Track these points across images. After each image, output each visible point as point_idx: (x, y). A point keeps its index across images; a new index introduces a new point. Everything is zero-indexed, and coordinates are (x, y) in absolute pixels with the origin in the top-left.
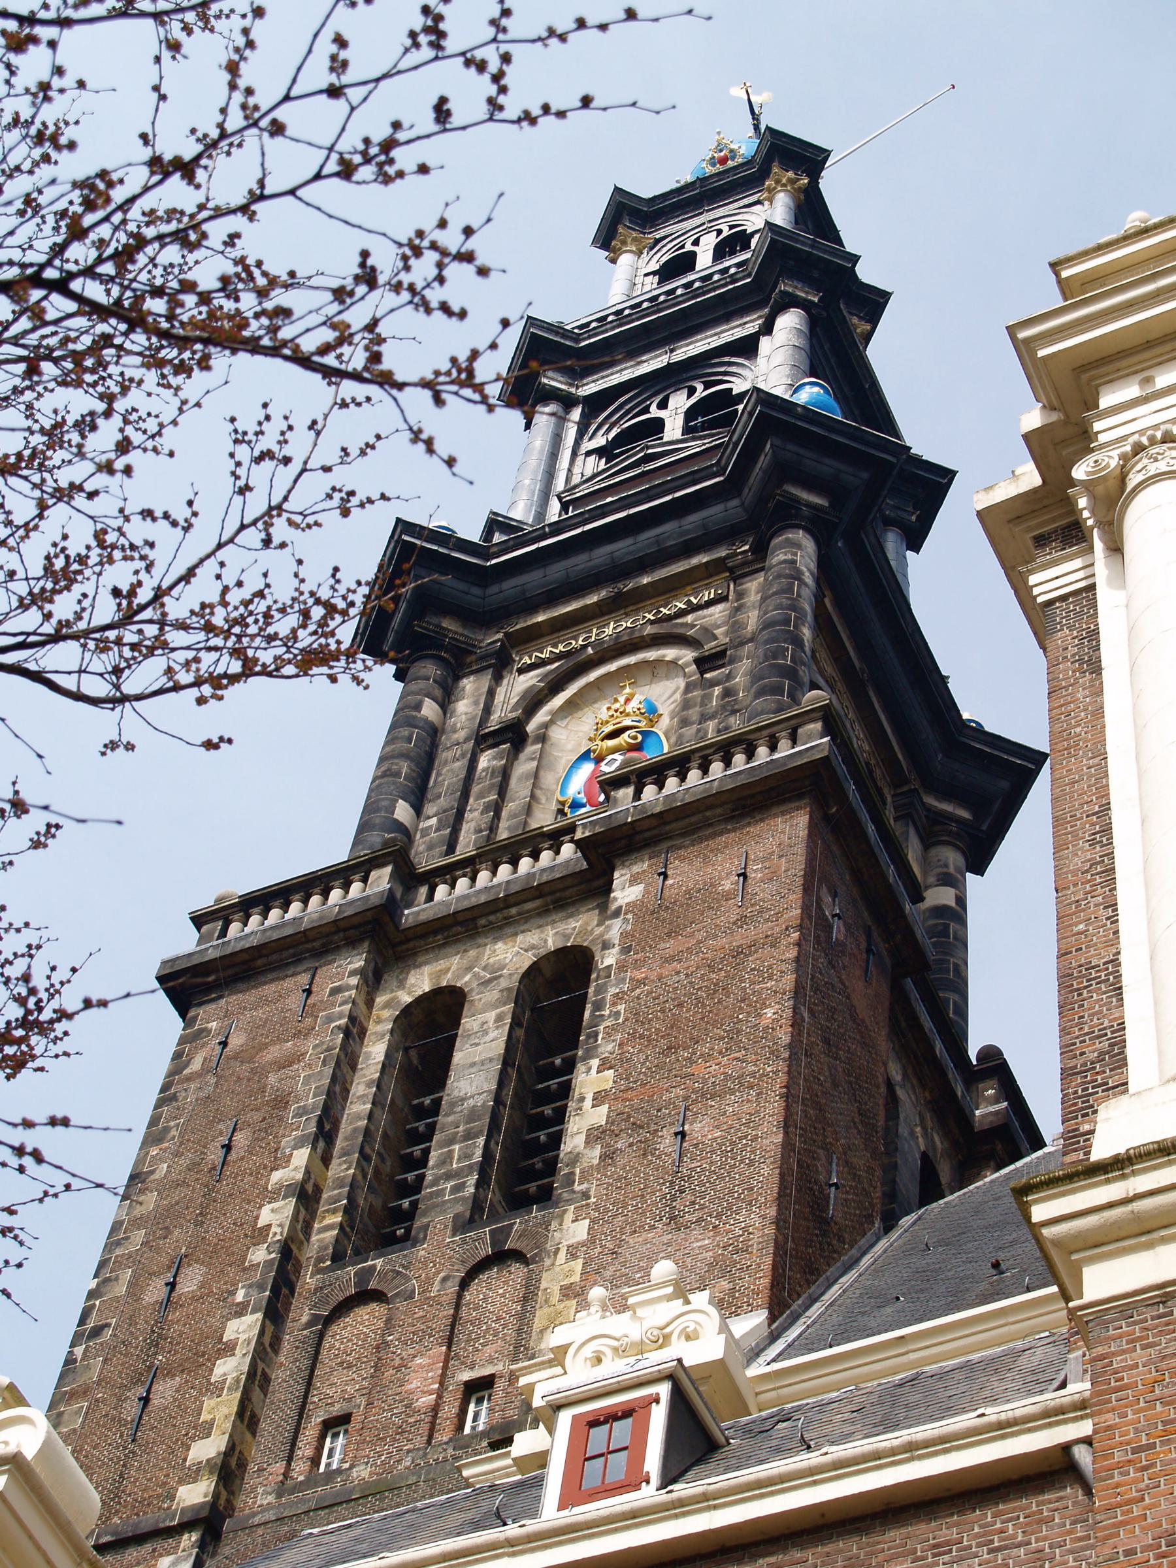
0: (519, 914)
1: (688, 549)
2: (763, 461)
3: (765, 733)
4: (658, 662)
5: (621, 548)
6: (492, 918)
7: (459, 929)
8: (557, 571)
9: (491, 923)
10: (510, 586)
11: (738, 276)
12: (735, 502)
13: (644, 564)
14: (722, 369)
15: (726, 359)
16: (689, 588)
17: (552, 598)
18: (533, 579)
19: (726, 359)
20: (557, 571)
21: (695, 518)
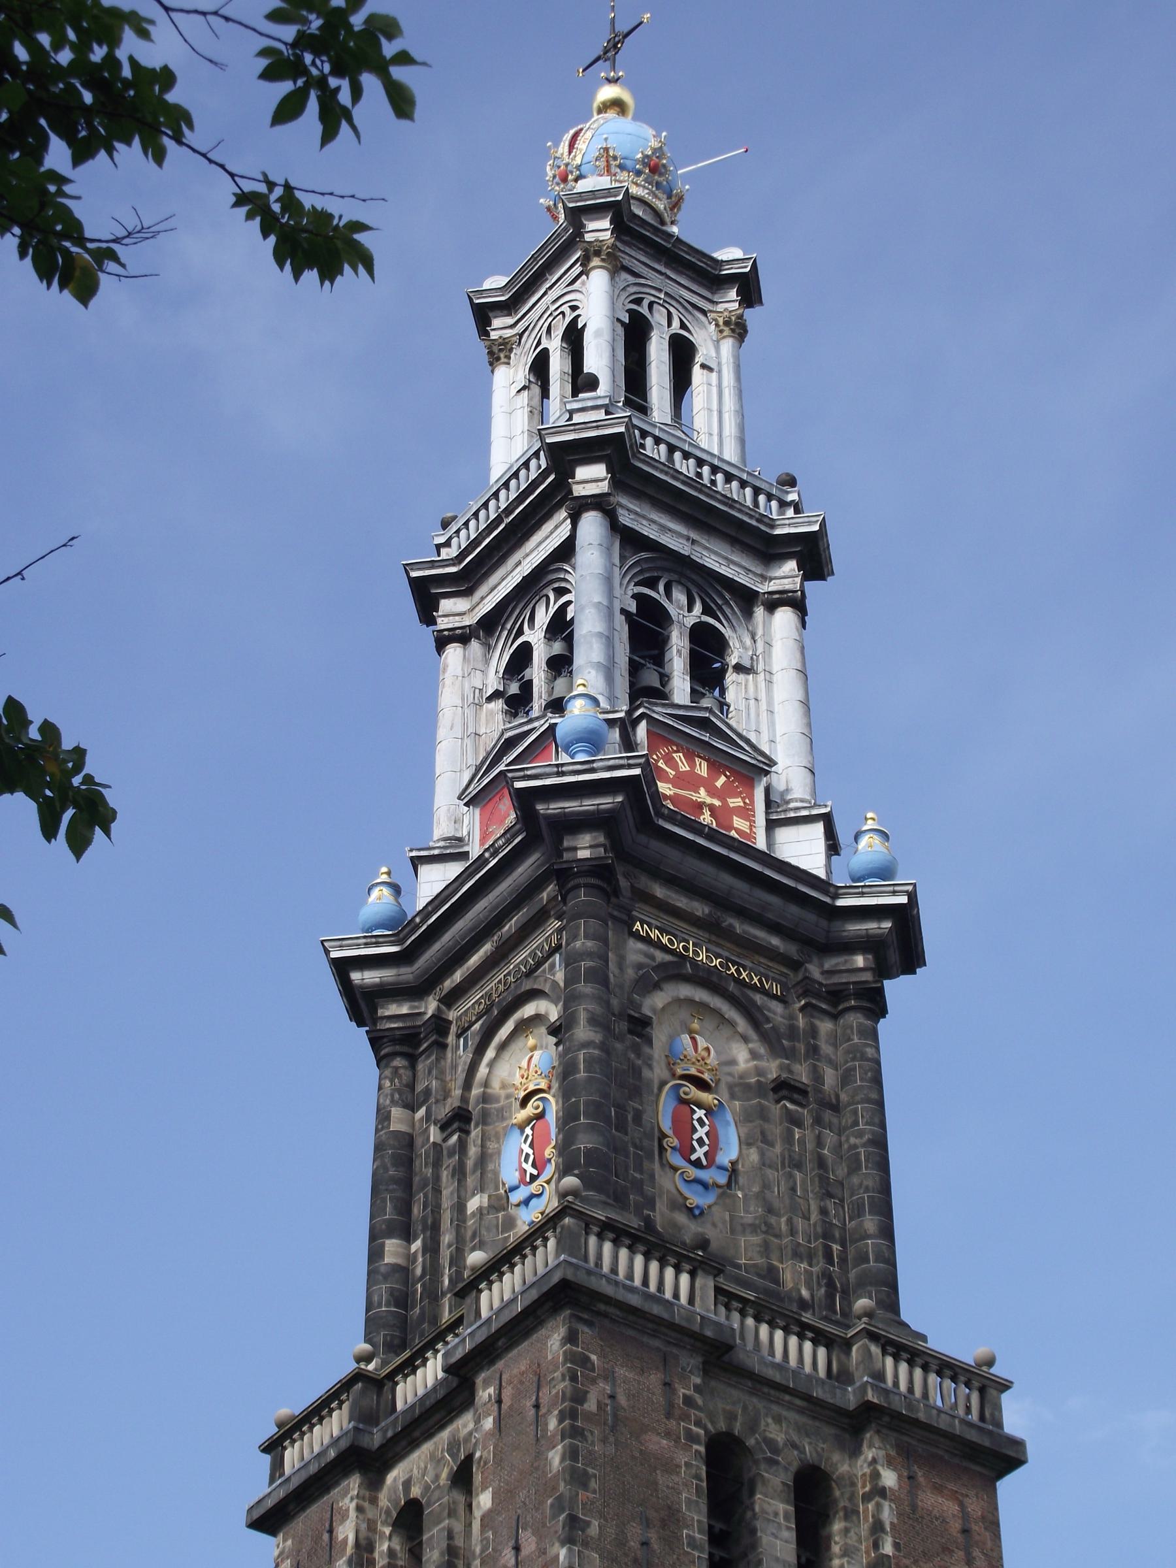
0: (789, 1402)
1: (775, 928)
2: (871, 926)
3: (968, 1375)
4: (732, 1024)
5: (740, 886)
6: (772, 1392)
7: (750, 1384)
8: (693, 866)
9: (769, 1394)
10: (657, 846)
11: (766, 520)
12: (824, 923)
13: (743, 913)
14: (720, 602)
15: (728, 596)
16: (757, 957)
17: (672, 881)
18: (673, 855)
19: (728, 596)
20: (693, 866)
21: (794, 910)
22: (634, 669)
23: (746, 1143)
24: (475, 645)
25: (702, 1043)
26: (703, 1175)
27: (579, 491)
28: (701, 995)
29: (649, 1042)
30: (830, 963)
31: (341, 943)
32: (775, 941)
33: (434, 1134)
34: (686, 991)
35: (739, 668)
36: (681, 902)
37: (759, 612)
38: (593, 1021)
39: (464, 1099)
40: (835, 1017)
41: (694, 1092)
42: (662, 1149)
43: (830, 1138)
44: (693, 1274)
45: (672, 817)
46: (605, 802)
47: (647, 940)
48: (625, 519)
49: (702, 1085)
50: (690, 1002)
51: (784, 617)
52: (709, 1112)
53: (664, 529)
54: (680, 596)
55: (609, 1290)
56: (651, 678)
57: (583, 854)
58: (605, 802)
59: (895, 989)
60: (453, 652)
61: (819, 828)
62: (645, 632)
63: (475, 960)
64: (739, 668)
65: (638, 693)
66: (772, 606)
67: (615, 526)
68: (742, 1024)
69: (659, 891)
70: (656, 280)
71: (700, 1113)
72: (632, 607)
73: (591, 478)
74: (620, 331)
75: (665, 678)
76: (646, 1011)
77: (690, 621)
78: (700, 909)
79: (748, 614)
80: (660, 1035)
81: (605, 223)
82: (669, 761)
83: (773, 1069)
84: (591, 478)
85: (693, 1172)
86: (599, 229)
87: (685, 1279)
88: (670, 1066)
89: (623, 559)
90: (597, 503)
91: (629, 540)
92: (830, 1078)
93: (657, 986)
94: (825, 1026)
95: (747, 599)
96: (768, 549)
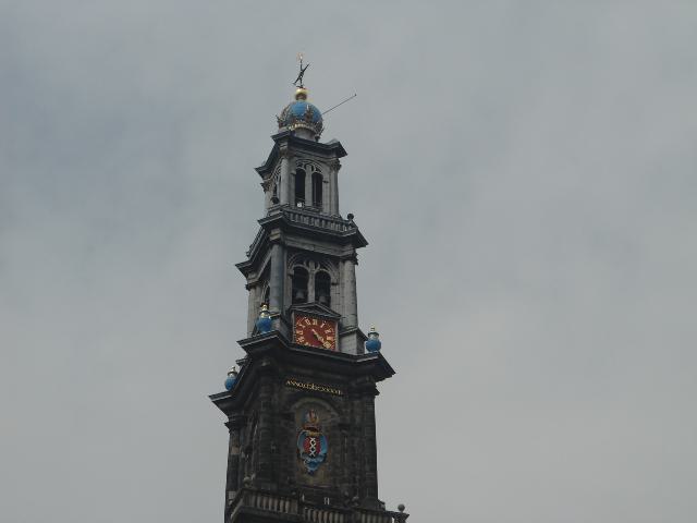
4: (324, 407)
22: (294, 293)
23: (330, 446)
24: (258, 289)
25: (313, 415)
26: (314, 460)
27: (272, 239)
28: (313, 400)
29: (293, 420)
30: (359, 380)
31: (219, 395)
32: (339, 377)
33: (243, 455)
34: (307, 400)
35: (333, 284)
36: (304, 371)
37: (341, 263)
38: (265, 420)
39: (251, 443)
40: (360, 398)
41: (311, 433)
42: (299, 455)
43: (357, 440)
44: (290, 501)
45: (295, 345)
46: (268, 347)
47: (291, 386)
48: (289, 244)
49: (313, 430)
50: (308, 403)
51: (348, 264)
52: (317, 439)
53: (304, 244)
54: (312, 265)
55: (256, 513)
56: (300, 295)
57: (264, 364)
58: (268, 347)
59: (379, 385)
60: (252, 290)
61: (355, 336)
62: (300, 280)
63: (250, 397)
64: (333, 284)
65: (295, 301)
66: (344, 262)
67: (284, 246)
68: (328, 407)
69: (295, 370)
70: (308, 157)
71: (313, 439)
72: (292, 272)
73: (276, 234)
74: (293, 178)
75: (306, 295)
76: (292, 410)
77: (316, 271)
78: (310, 372)
79: (337, 265)
80: (298, 418)
81: (286, 143)
82: (303, 323)
83: (338, 419)
84: (276, 234)
85: (309, 460)
86: (284, 146)
87: (287, 504)
88: (303, 425)
89: (288, 257)
90: (277, 242)
91: (289, 250)
92: (358, 419)
93: (297, 400)
94: (357, 402)
95: (336, 261)
96: (339, 241)
